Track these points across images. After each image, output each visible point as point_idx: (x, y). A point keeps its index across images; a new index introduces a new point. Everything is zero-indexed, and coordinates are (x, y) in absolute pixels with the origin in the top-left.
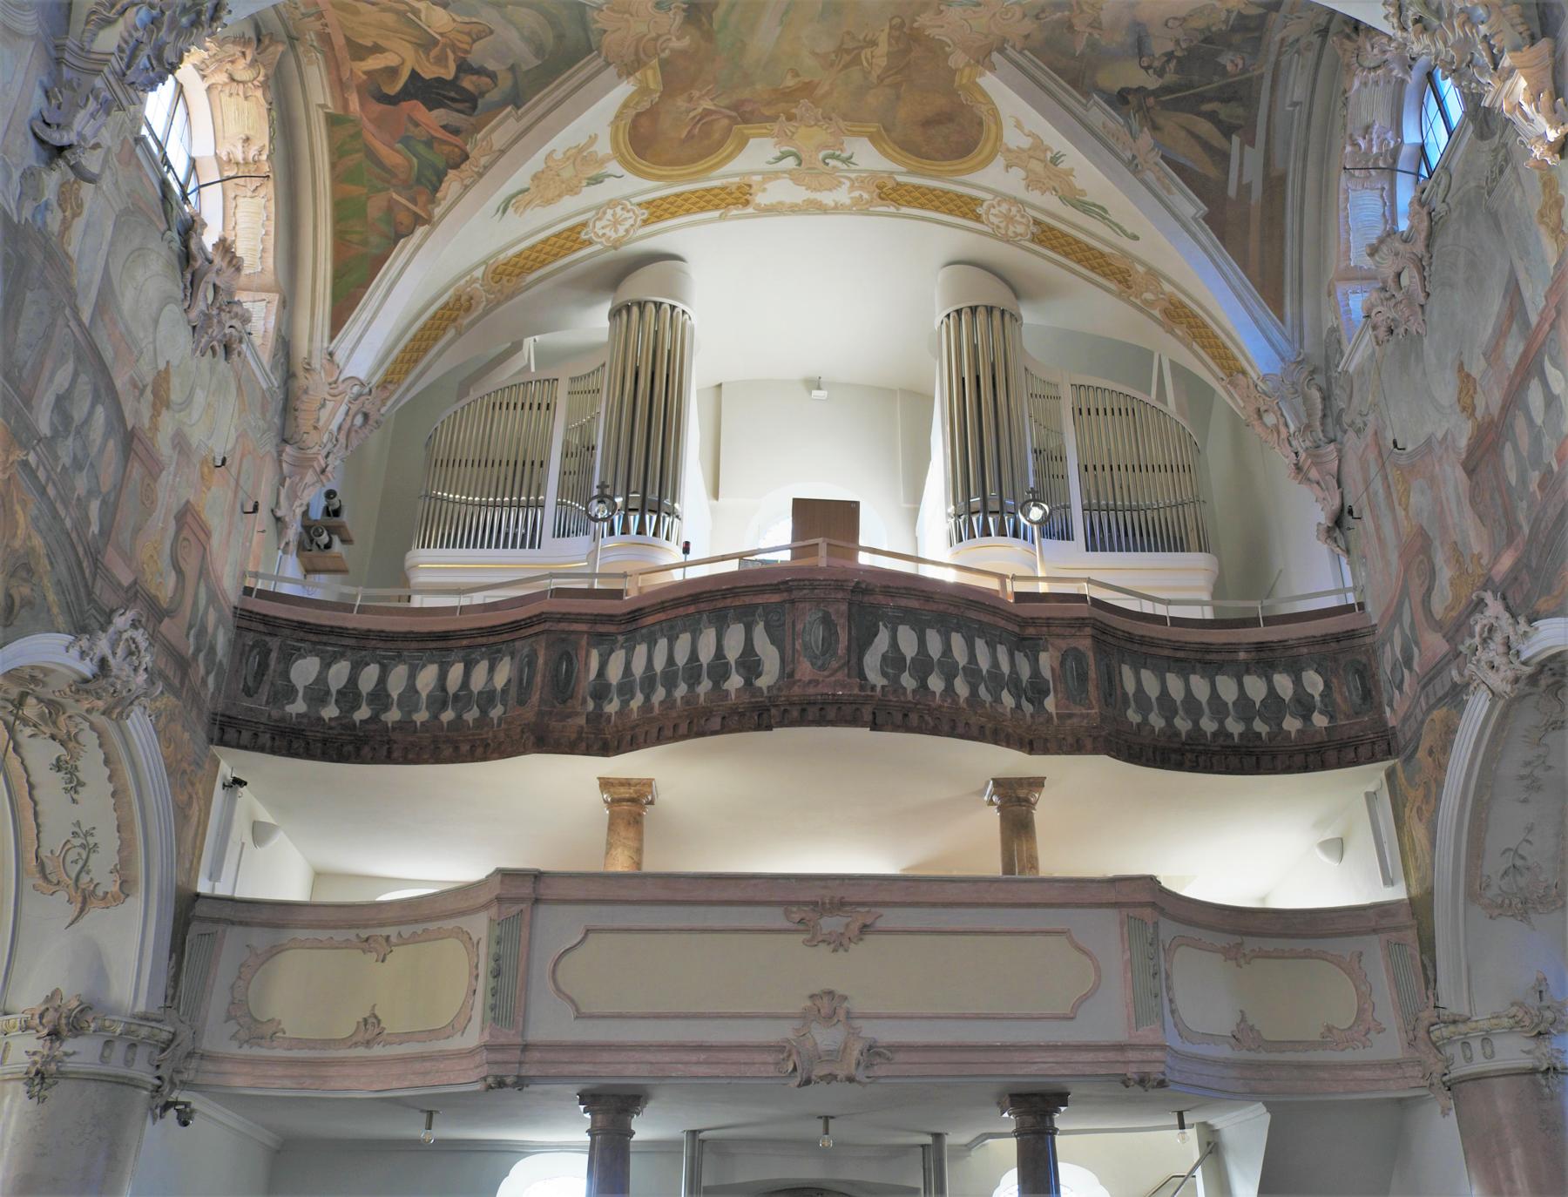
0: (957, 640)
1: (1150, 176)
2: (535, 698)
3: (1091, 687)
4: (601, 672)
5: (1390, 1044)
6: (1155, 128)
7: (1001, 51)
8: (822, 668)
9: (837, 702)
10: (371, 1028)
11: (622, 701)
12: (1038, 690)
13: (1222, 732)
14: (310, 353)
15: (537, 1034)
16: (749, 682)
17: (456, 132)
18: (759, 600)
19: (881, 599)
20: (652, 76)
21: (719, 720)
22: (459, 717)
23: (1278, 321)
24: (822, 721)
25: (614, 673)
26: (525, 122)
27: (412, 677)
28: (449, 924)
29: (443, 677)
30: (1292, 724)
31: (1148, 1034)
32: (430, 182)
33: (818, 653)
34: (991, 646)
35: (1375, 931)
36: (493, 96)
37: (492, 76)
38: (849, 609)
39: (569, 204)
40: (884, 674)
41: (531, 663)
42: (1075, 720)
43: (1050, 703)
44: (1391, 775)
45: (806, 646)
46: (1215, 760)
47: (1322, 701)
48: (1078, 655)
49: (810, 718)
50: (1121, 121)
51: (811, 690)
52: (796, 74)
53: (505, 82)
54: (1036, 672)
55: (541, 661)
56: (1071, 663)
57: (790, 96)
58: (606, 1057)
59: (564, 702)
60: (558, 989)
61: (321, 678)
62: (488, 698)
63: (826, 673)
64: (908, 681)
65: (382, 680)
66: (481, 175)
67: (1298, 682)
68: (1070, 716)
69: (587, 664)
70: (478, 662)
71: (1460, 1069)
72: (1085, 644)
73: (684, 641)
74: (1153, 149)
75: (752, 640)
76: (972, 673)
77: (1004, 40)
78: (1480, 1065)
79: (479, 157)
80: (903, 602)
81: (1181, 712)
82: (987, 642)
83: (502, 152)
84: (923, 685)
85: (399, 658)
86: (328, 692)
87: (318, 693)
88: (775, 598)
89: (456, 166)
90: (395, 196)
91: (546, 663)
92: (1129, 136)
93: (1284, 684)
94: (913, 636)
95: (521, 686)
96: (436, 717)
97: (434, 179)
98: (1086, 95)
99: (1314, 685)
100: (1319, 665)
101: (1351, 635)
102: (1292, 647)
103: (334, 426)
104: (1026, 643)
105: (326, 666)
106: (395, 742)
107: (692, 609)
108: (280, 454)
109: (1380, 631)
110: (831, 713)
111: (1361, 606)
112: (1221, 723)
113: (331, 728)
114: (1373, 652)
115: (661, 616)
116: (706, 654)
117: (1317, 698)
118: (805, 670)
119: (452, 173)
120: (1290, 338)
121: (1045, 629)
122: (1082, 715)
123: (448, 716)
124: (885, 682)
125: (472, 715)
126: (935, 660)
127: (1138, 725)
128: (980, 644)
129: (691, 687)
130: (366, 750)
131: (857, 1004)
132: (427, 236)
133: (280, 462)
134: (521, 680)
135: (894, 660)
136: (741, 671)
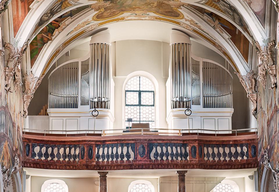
0: (169, 148)
1: (218, 30)
3: (197, 155)
7: (183, 6)
8: (142, 157)
9: (145, 165)
11: (103, 159)
12: (186, 155)
13: (225, 160)
14: (27, 71)
16: (128, 159)
18: (129, 142)
19: (154, 142)
20: (102, 10)
21: (122, 167)
22: (69, 160)
23: (246, 63)
24: (142, 168)
25: (101, 153)
26: (73, 19)
27: (58, 150)
30: (239, 158)
32: (51, 32)
33: (141, 154)
38: (148, 144)
40: (154, 157)
41: (84, 150)
42: (193, 162)
43: (188, 158)
44: (258, 169)
45: (139, 152)
46: (222, 167)
47: (246, 154)
48: (194, 147)
49: (140, 168)
50: (211, 18)
51: (140, 162)
54: (186, 151)
55: (86, 150)
59: (91, 159)
61: (40, 151)
62: (75, 156)
63: (143, 158)
64: (159, 158)
65: (52, 151)
66: (63, 30)
67: (242, 149)
68: (192, 161)
69: (95, 151)
70: (72, 148)
72: (196, 145)
73: (115, 148)
74: (219, 24)
75: (128, 150)
76: (172, 155)
77: (184, 4)
80: (159, 142)
81: (216, 156)
82: (175, 147)
83: (68, 25)
84: (162, 159)
85: (55, 146)
86: (42, 154)
87: (40, 154)
88: (133, 142)
90: (43, 35)
91: (87, 150)
92: (213, 21)
93: (239, 149)
95: (82, 155)
96: (64, 160)
97: (52, 31)
98: (203, 14)
99: (245, 150)
100: (247, 145)
101: (254, 140)
102: (242, 141)
104: (184, 145)
105: (41, 148)
106: (57, 165)
107: (116, 142)
108: (23, 96)
109: (259, 140)
110: (144, 167)
111: (257, 132)
113: (44, 162)
114: (258, 144)
115: (110, 143)
116: (119, 153)
117: (245, 153)
120: (249, 67)
121: (188, 142)
122: (195, 160)
123: (67, 160)
124: (155, 159)
125: (72, 160)
126: (165, 153)
127: (207, 160)
128: (174, 148)
130: (51, 167)
132: (51, 43)
133: (23, 98)
134: (82, 153)
135: (156, 154)
136: (126, 157)
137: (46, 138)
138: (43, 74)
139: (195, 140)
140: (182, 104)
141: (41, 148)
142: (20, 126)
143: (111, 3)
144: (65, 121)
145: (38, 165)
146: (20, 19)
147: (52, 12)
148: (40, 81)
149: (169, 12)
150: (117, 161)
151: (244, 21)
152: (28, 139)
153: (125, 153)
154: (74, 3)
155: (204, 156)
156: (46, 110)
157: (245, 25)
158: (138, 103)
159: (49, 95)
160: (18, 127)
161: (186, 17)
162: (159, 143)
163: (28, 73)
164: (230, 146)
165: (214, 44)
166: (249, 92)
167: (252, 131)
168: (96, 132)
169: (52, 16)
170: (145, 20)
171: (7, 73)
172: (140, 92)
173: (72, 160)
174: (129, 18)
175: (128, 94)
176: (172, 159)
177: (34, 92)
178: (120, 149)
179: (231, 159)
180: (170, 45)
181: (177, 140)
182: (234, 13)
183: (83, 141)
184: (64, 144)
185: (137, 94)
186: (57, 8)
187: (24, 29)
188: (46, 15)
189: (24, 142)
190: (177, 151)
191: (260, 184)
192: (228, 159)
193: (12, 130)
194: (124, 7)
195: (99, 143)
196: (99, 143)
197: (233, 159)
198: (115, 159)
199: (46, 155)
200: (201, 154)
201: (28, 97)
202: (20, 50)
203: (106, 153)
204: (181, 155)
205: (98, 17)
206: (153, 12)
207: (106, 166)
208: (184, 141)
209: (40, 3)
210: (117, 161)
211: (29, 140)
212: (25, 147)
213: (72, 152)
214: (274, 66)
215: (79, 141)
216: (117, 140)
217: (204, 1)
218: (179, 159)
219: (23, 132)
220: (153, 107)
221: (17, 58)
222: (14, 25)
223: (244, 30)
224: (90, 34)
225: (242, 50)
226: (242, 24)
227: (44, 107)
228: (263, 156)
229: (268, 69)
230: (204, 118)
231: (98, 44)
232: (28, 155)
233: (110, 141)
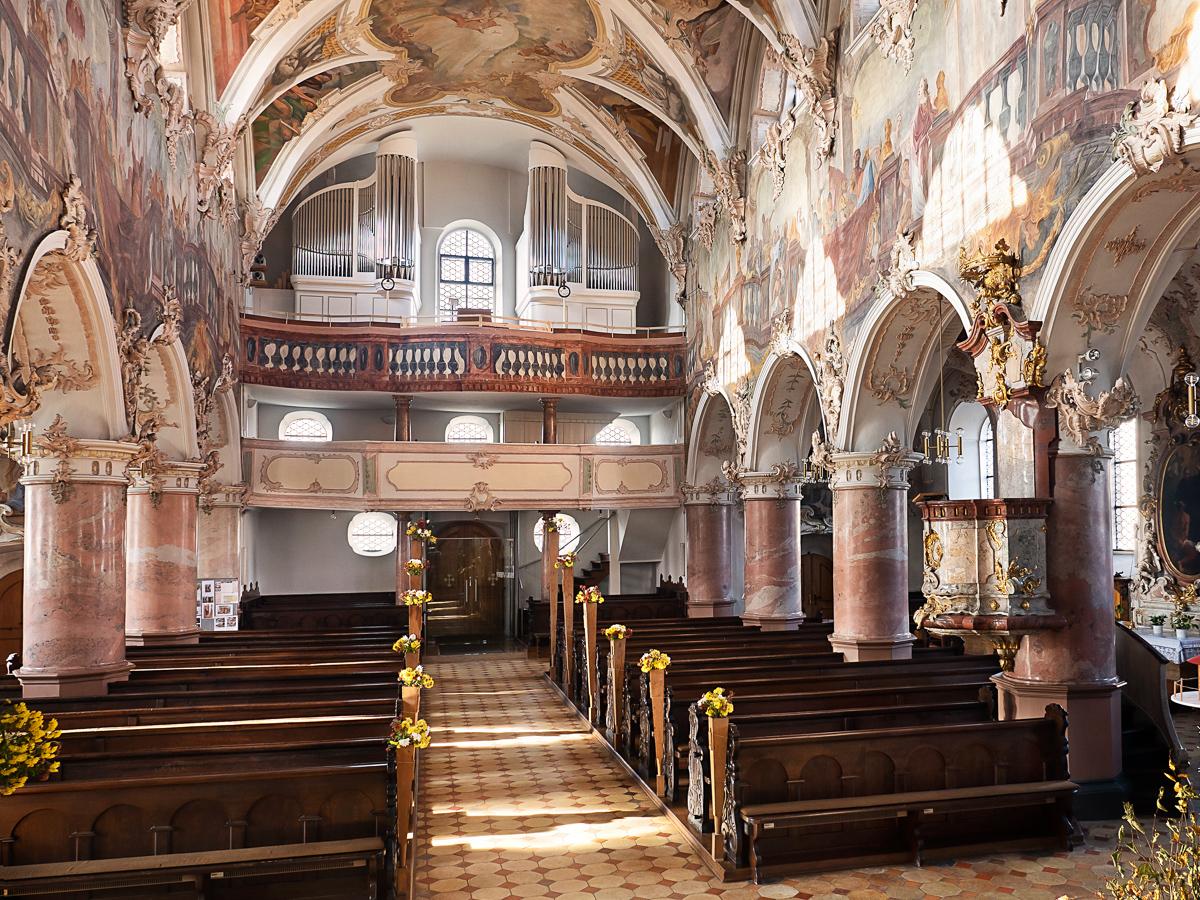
0: (530, 354)
1: (623, 141)
2: (368, 368)
3: (579, 368)
4: (394, 359)
5: (670, 492)
6: (627, 121)
7: (562, 86)
8: (481, 368)
10: (316, 486)
12: (560, 369)
13: (628, 380)
15: (382, 497)
16: (453, 372)
17: (311, 96)
18: (456, 340)
20: (405, 81)
22: (336, 372)
25: (399, 360)
26: (344, 95)
27: (315, 353)
28: (345, 454)
29: (327, 353)
30: (653, 378)
31: (586, 496)
34: (543, 355)
35: (671, 454)
36: (330, 83)
37: (330, 76)
39: (361, 119)
41: (365, 352)
43: (564, 374)
45: (474, 359)
48: (576, 355)
51: (476, 378)
52: (470, 80)
53: (336, 79)
54: (559, 361)
55: (369, 353)
56: (573, 358)
57: (469, 85)
58: (407, 503)
60: (390, 482)
61: (277, 352)
62: (348, 365)
64: (512, 372)
65: (302, 353)
67: (658, 362)
71: (689, 502)
72: (578, 350)
78: (695, 501)
79: (322, 106)
80: (511, 341)
83: (333, 106)
84: (517, 373)
85: (308, 345)
86: (281, 358)
87: (277, 359)
88: (463, 340)
89: (312, 111)
94: (514, 354)
95: (362, 364)
101: (679, 346)
103: (262, 231)
105: (278, 348)
112: (628, 378)
114: (687, 353)
115: (417, 340)
116: (436, 359)
118: (474, 369)
119: (309, 114)
123: (331, 371)
125: (342, 371)
129: (431, 372)
131: (490, 487)
135: (507, 365)
137: (287, 328)
138: (282, 205)
139: (578, 342)
140: (549, 278)
141: (278, 348)
142: (233, 298)
143: (423, 65)
144: (326, 300)
145: (273, 379)
146: (230, 59)
147: (302, 58)
148: (276, 218)
149: (534, 99)
150: (431, 376)
151: (691, 109)
152: (251, 328)
153: (447, 360)
154: (348, 49)
155: (592, 372)
156: (288, 280)
157: (691, 117)
158: (463, 279)
159: (294, 250)
160: (230, 302)
161: (564, 112)
162: (512, 344)
163: (251, 200)
164: (636, 357)
165: (612, 170)
166: (671, 261)
167: (670, 331)
168: (390, 321)
169: (301, 68)
170: (485, 116)
171: (201, 177)
172: (467, 259)
173: (342, 371)
174: (455, 109)
175: (446, 262)
176: (536, 374)
177: (263, 239)
178: (437, 353)
179: (638, 379)
180: (529, 169)
181: (545, 340)
182: (672, 94)
183: (364, 336)
184: (325, 341)
185: (461, 263)
186: (313, 50)
187: (240, 83)
188: (289, 62)
189: (242, 334)
190: (544, 361)
191: (690, 425)
192: (632, 379)
193: (215, 301)
194: (448, 79)
195: (397, 341)
196: (397, 341)
197: (642, 379)
198: (427, 372)
199: (290, 360)
200: (587, 368)
201: (250, 248)
202: (231, 129)
203: (409, 359)
204: (551, 368)
205: (396, 96)
206: (503, 99)
207: (409, 384)
208: (557, 342)
209: (273, 29)
210: (431, 376)
211: (254, 330)
212: (245, 343)
213: (343, 358)
214: (742, 199)
215: (357, 336)
216: (431, 336)
217: (610, 71)
218: (548, 374)
219: (241, 315)
220: (491, 288)
221: (225, 145)
222: (216, 73)
223: (686, 129)
224: (373, 138)
225: (664, 178)
226: (683, 117)
227: (284, 274)
228: (699, 374)
229: (730, 206)
230: (589, 307)
231: (392, 156)
232: (251, 360)
233: (418, 336)
